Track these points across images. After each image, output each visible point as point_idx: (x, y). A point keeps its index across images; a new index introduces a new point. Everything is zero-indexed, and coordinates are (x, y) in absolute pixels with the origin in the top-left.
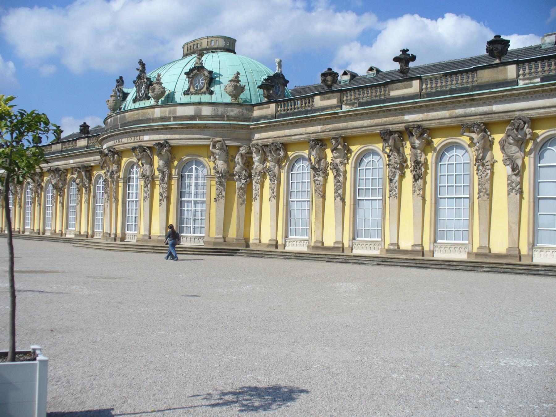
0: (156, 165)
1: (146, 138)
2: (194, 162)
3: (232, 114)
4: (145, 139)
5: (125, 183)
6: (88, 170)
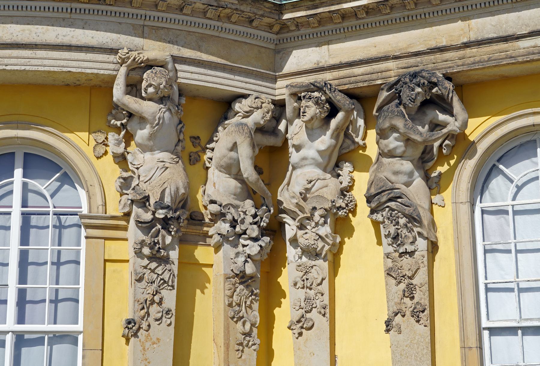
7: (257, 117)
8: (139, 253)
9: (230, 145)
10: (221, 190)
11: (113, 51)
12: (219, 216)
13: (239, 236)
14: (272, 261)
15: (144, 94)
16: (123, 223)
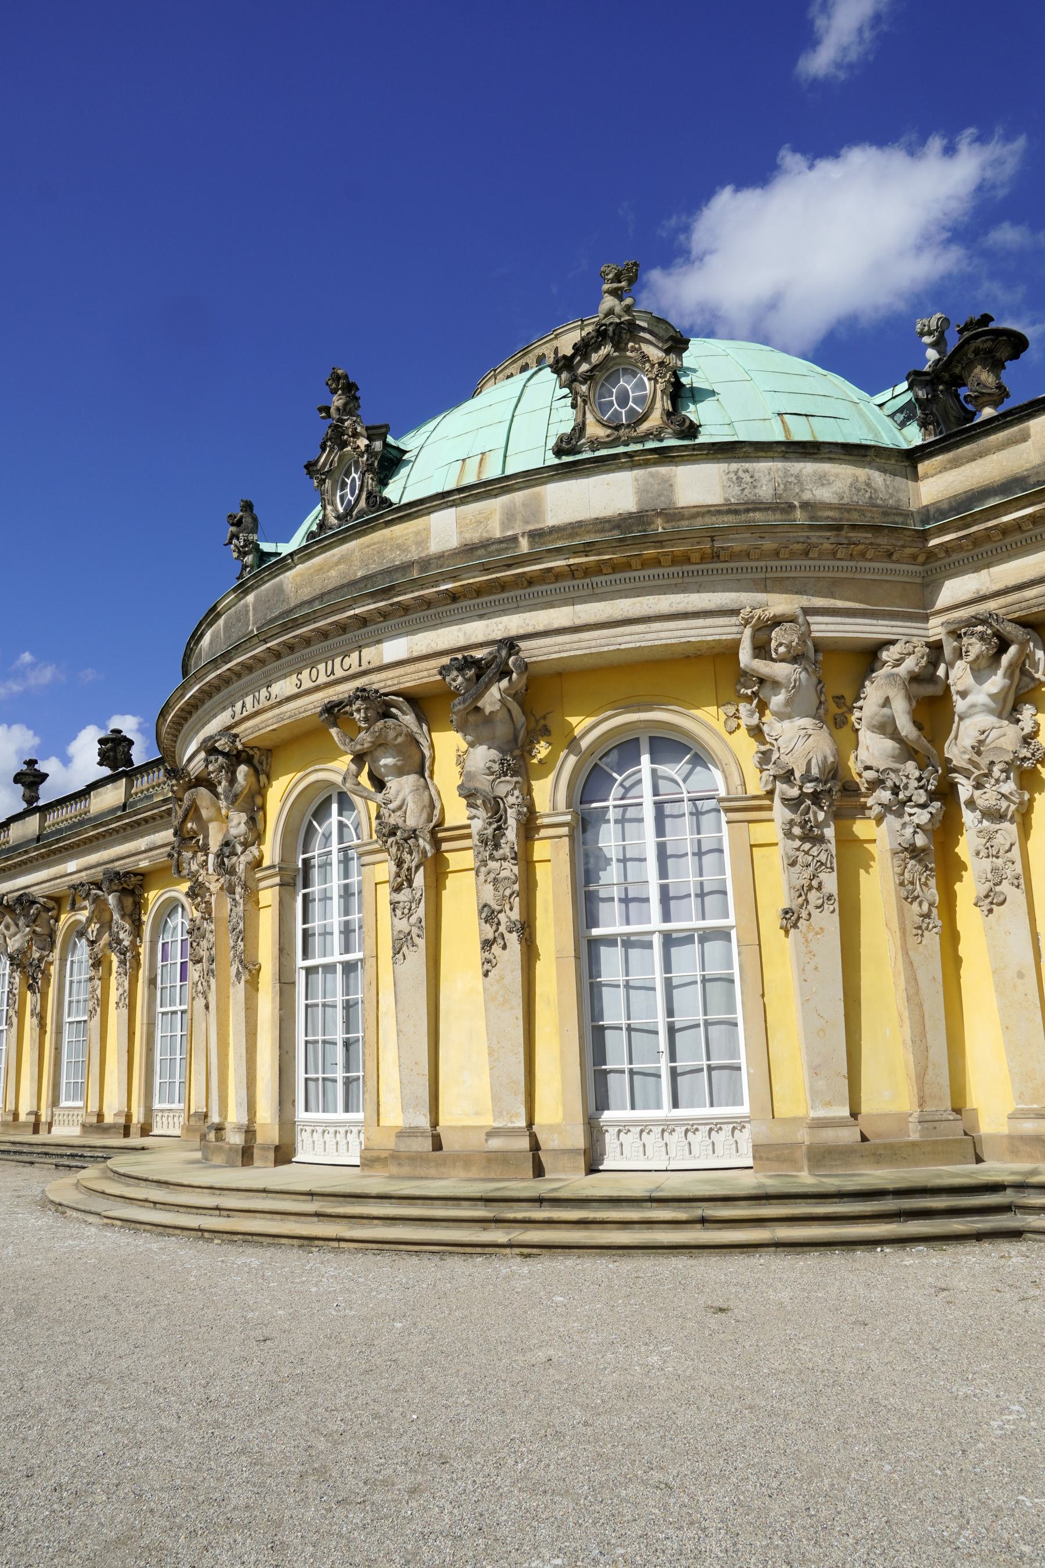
0: (446, 777)
1: (394, 649)
2: (645, 745)
3: (824, 494)
4: (387, 659)
5: (287, 885)
6: (130, 886)
7: (910, 664)
8: (788, 835)
9: (881, 701)
10: (876, 753)
11: (734, 612)
12: (877, 784)
13: (903, 804)
14: (946, 829)
15: (774, 656)
16: (767, 802)
